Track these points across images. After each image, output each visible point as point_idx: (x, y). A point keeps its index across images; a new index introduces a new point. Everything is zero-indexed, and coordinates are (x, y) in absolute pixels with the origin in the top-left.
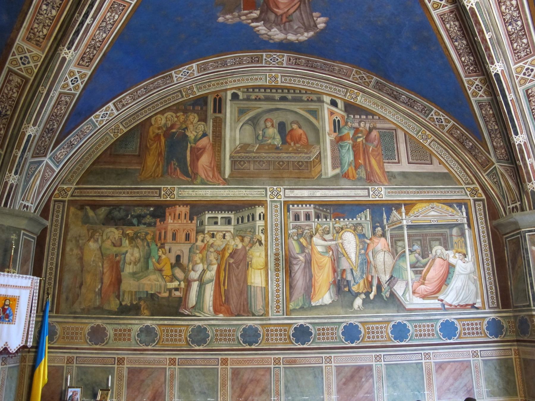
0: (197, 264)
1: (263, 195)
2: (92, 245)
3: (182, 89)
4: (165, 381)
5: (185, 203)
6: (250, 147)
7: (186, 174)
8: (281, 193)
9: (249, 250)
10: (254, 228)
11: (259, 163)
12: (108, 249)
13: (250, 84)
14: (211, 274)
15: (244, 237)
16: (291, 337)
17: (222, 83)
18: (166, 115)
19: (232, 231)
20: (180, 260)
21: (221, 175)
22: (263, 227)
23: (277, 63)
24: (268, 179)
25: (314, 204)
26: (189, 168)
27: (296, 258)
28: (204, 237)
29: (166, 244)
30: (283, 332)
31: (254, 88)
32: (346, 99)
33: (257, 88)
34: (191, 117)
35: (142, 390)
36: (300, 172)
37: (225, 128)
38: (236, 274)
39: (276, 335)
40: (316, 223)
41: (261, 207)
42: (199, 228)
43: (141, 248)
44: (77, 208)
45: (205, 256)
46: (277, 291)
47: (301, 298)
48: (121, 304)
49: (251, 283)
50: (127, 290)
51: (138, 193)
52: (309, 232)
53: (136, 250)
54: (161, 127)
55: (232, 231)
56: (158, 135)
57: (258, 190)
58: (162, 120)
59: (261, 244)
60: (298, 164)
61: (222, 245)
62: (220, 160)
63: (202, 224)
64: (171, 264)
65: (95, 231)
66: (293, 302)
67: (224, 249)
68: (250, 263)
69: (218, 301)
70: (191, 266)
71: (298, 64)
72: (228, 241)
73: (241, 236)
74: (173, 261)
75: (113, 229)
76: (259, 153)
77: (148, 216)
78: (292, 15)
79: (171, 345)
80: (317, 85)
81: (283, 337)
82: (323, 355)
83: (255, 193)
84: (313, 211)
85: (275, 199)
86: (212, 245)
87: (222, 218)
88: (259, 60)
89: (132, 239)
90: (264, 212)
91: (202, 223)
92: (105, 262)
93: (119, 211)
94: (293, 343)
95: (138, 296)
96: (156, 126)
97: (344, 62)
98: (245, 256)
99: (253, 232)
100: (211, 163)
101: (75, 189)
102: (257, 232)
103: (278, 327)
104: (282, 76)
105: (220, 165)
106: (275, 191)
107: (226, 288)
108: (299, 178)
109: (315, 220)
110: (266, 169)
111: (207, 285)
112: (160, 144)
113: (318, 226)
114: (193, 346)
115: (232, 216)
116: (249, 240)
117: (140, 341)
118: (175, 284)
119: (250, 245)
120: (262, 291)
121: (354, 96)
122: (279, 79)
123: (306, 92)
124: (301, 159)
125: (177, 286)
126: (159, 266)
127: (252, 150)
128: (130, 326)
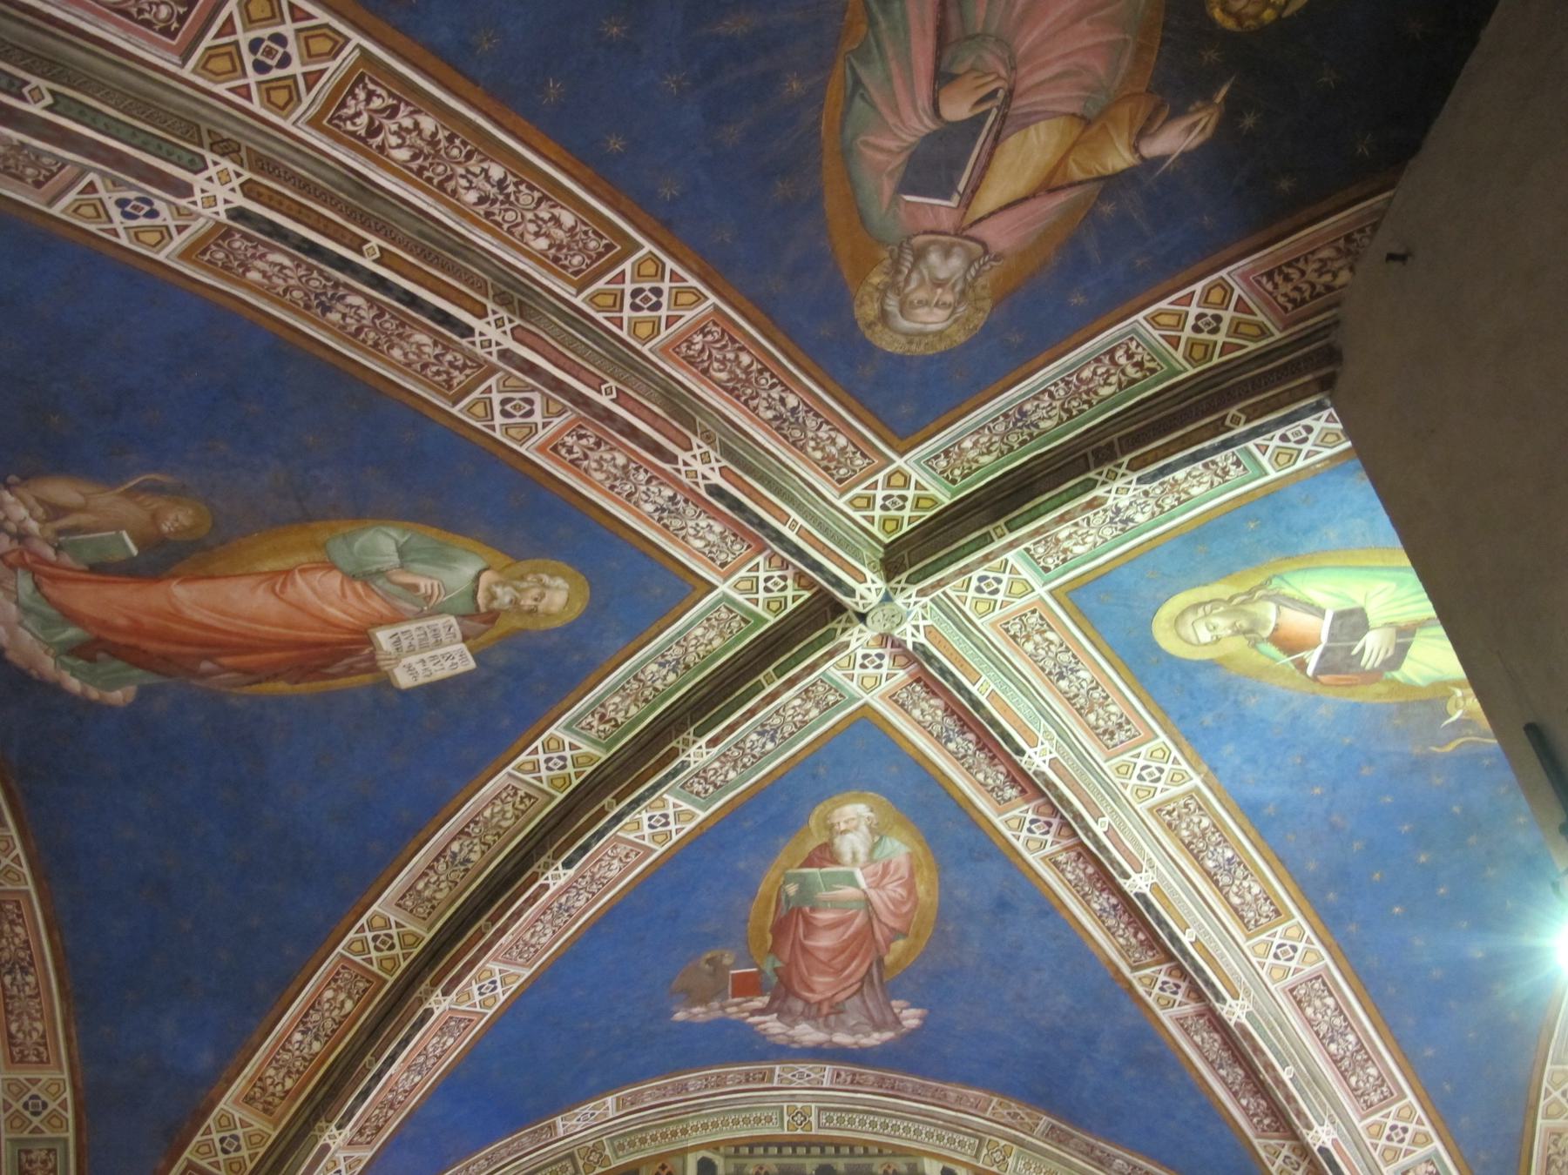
3: (576, 1149)
13: (743, 1134)
17: (674, 1134)
23: (809, 1082)
31: (752, 1143)
32: (980, 1165)
33: (759, 1145)
71: (859, 1083)
78: (843, 1002)
80: (907, 1129)
88: (765, 1076)
97: (969, 1082)
104: (820, 1110)
121: (998, 1156)
122: (813, 1119)
123: (880, 1151)
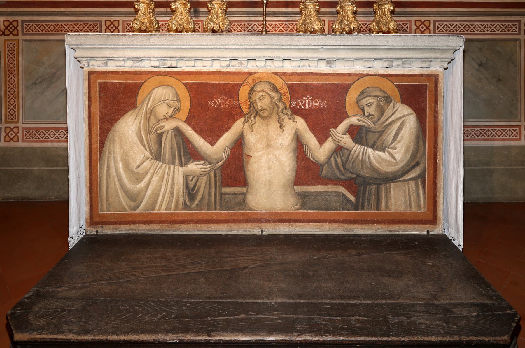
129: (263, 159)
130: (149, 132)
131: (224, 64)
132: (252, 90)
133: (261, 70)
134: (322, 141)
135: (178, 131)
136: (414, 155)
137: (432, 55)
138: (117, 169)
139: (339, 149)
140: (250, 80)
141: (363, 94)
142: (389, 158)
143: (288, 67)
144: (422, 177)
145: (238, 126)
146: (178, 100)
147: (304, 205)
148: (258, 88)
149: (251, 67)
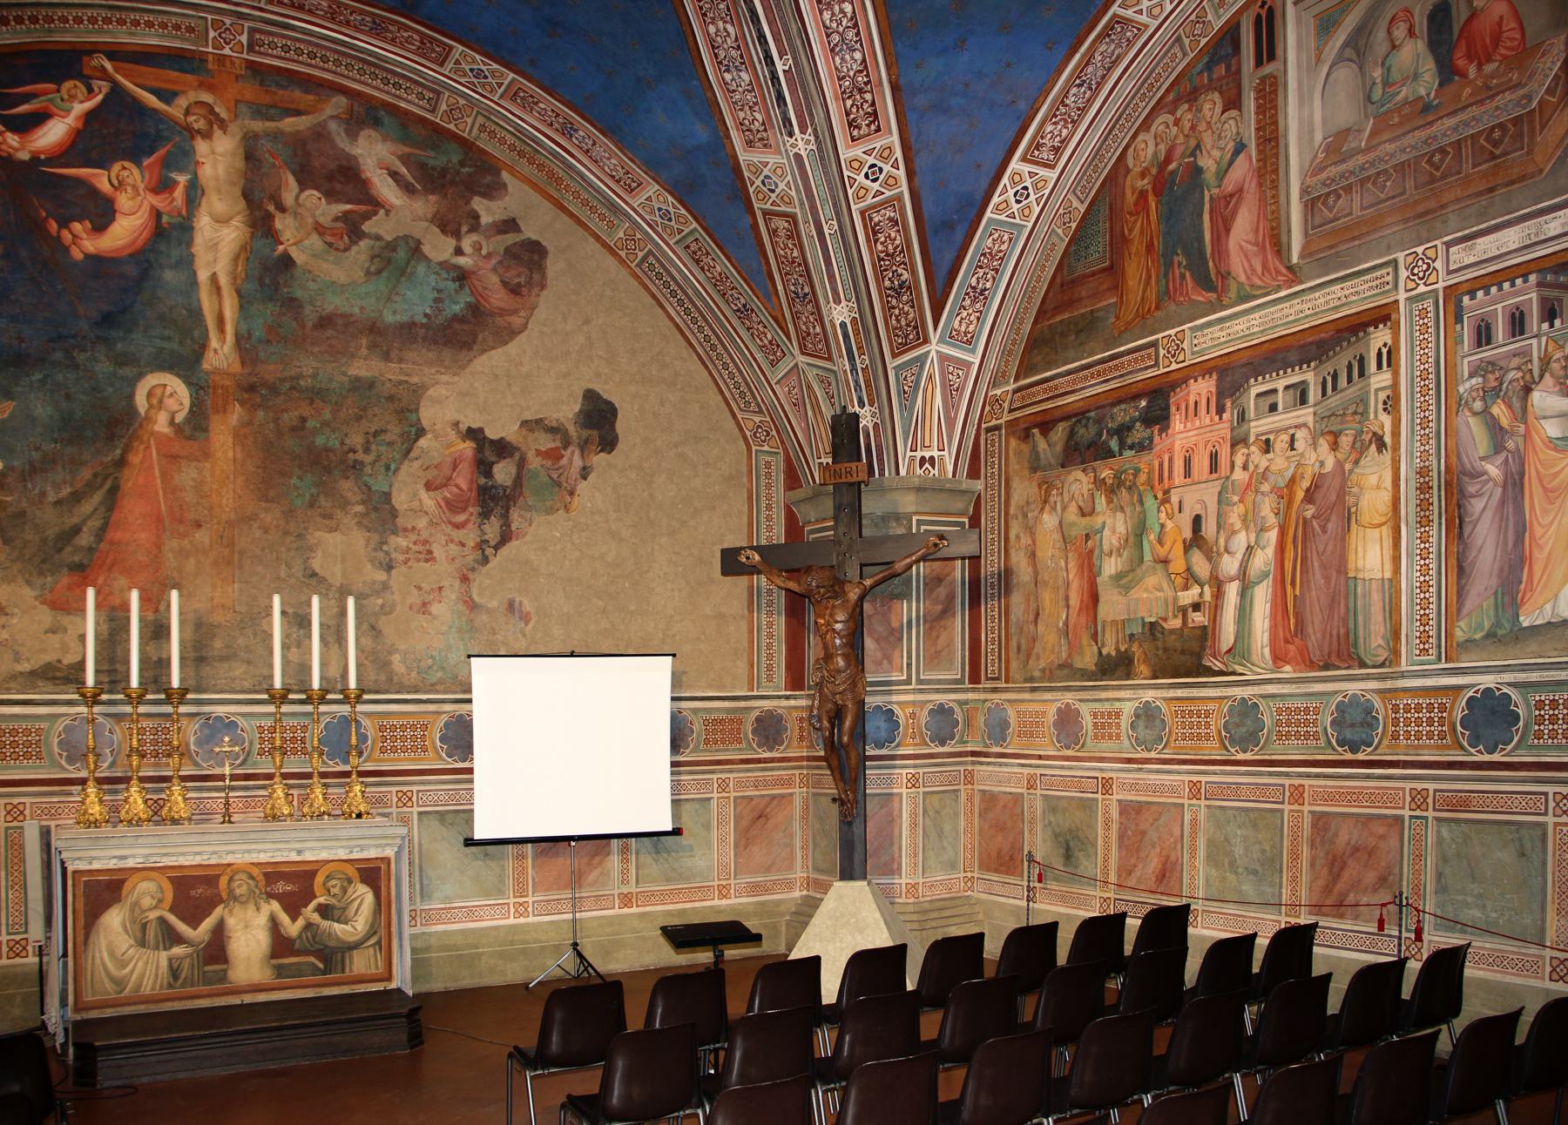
0: (1234, 533)
1: (1387, 287)
2: (1049, 520)
4: (1182, 836)
5: (1204, 369)
6: (1350, 138)
7: (1205, 283)
8: (1438, 264)
9: (1351, 471)
10: (1363, 401)
11: (1374, 183)
12: (1074, 524)
14: (1264, 558)
15: (1340, 432)
16: (1459, 728)
18: (1153, 128)
19: (1310, 420)
20: (1200, 531)
21: (1281, 261)
22: (1389, 392)
24: (1402, 227)
25: (1539, 271)
26: (1211, 264)
27: (1477, 475)
28: (1248, 455)
29: (1173, 491)
30: (1435, 715)
34: (1207, 106)
35: (1142, 854)
36: (1496, 165)
37: (1286, 104)
38: (1321, 548)
39: (1418, 722)
40: (1544, 339)
41: (1381, 326)
42: (1235, 433)
43: (1128, 510)
44: (1019, 438)
45: (1251, 507)
46: (1424, 587)
47: (1488, 604)
48: (1100, 653)
49: (1357, 570)
50: (1109, 619)
51: (1116, 368)
52: (1521, 374)
53: (1119, 515)
54: (1146, 168)
55: (1311, 425)
56: (1143, 195)
57: (1374, 275)
58: (1148, 149)
59: (1381, 446)
60: (1487, 140)
61: (1287, 469)
62: (1278, 212)
63: (1243, 419)
64: (1184, 541)
65: (1050, 487)
66: (1466, 620)
67: (1293, 480)
68: (1353, 510)
69: (1280, 629)
70: (1222, 542)
72: (1302, 455)
73: (1331, 432)
74: (1188, 534)
75: (1078, 474)
76: (1375, 147)
77: (1138, 424)
79: (1191, 748)
81: (1436, 728)
82: (1550, 789)
83: (1366, 286)
84: (1534, 296)
85: (1422, 289)
86: (1264, 476)
87: (1287, 388)
89: (1111, 491)
90: (1389, 342)
91: (1242, 417)
92: (1070, 555)
93: (1086, 426)
94: (1462, 748)
95: (1128, 632)
96: (1138, 169)
98: (1342, 493)
99: (1362, 414)
100: (1257, 231)
101: (1015, 391)
102: (1372, 410)
103: (1424, 697)
105: (1278, 227)
106: (1420, 263)
107: (1298, 592)
108: (1491, 190)
109: (1539, 328)
110: (1393, 197)
111: (1256, 588)
112: (1148, 217)
113: (1550, 350)
114: (1233, 750)
115: (1309, 377)
116: (1351, 439)
117: (1137, 739)
118: (1188, 596)
119: (1353, 456)
120: (1384, 592)
124: (1498, 117)
125: (1197, 599)
126: (1162, 552)
127: (1353, 145)
128: (1117, 704)
129: (243, 938)
130: (133, 922)
131: (205, 857)
132: (231, 879)
133: (239, 861)
134: (294, 919)
135: (162, 920)
136: (372, 926)
137: (384, 842)
138: (102, 958)
139: (309, 926)
140: (229, 870)
141: (329, 877)
142: (352, 930)
143: (263, 858)
144: (379, 943)
145: (219, 911)
146: (162, 892)
147: (279, 976)
148: (236, 877)
149: (229, 859)
